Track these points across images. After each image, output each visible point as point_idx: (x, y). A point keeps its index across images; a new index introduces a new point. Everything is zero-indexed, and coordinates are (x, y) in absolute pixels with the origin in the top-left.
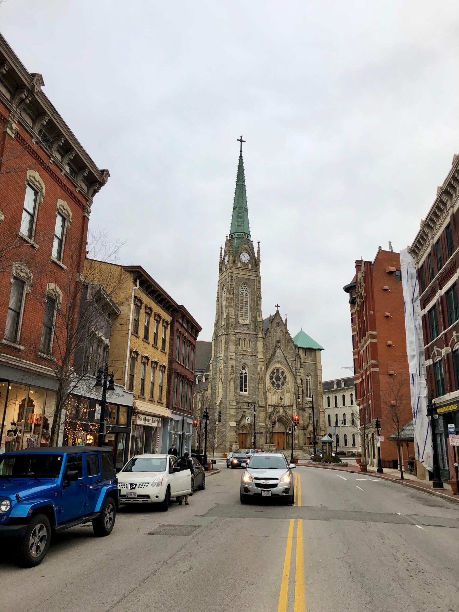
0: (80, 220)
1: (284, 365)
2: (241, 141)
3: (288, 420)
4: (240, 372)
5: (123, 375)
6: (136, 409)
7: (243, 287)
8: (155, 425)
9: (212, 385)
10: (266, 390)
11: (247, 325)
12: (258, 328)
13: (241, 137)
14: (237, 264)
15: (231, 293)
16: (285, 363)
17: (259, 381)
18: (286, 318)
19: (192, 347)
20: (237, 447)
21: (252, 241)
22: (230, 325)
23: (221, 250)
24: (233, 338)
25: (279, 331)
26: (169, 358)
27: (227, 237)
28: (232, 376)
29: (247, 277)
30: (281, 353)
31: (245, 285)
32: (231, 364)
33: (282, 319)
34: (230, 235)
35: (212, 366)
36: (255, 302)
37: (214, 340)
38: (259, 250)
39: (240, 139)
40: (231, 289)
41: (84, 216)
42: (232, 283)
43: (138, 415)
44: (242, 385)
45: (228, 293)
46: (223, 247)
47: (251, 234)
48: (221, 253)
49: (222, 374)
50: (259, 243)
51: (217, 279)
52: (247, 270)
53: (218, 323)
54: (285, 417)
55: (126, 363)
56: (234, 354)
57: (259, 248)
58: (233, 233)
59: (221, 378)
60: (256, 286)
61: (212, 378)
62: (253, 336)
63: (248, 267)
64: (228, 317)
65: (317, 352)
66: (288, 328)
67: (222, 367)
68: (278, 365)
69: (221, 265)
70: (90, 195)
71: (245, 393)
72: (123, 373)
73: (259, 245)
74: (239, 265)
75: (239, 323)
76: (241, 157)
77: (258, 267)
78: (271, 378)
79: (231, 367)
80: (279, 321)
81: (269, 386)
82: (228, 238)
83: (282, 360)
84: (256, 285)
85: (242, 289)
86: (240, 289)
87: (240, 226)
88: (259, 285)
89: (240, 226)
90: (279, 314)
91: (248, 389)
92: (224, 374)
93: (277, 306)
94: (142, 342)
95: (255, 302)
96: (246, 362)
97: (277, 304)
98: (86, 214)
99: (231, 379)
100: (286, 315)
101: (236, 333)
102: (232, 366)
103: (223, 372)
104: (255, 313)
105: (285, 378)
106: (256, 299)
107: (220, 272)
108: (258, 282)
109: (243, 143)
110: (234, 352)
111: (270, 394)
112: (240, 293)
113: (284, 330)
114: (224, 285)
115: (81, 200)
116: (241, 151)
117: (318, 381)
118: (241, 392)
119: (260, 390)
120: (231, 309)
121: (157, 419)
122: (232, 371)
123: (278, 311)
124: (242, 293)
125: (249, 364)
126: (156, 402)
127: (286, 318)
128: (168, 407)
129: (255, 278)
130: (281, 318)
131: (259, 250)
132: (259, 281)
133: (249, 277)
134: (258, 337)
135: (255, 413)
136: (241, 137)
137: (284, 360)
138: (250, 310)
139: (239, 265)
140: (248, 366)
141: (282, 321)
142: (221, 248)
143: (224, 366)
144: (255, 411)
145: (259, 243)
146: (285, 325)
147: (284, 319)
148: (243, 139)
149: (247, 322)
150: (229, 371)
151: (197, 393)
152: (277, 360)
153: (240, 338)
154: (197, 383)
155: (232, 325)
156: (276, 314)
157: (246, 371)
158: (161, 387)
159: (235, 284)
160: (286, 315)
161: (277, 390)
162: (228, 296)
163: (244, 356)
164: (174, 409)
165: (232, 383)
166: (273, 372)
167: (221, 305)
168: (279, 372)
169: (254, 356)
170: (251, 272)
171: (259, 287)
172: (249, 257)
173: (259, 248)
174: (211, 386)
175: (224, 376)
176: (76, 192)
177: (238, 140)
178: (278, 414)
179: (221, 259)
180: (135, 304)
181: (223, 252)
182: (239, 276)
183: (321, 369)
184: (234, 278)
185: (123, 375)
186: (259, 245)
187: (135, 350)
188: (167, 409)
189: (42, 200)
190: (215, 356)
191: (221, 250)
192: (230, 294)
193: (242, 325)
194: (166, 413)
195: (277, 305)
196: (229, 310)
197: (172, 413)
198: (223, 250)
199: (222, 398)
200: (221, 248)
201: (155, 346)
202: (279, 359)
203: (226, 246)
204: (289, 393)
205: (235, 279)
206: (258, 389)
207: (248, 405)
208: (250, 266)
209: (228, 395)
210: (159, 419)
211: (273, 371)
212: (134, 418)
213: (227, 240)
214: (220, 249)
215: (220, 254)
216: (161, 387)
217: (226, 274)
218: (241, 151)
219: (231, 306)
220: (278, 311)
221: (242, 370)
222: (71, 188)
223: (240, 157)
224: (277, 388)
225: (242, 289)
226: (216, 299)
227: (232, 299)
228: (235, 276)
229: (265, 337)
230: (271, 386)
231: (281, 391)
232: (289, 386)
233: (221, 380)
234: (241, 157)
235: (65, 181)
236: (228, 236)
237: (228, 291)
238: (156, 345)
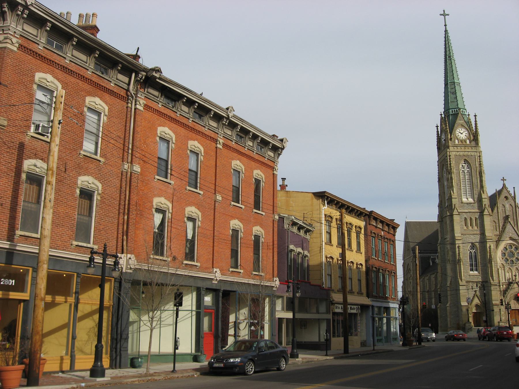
0: (272, 177)
2: (444, 15)
4: (469, 252)
5: (322, 276)
6: (334, 300)
7: (464, 165)
8: (354, 311)
10: (499, 268)
11: (471, 203)
13: (444, 11)
14: (454, 141)
18: (514, 191)
19: (392, 243)
21: (469, 115)
23: (437, 129)
26: (365, 257)
27: (441, 115)
29: (466, 153)
33: (510, 192)
34: (444, 112)
35: (440, 248)
38: (476, 124)
39: (442, 13)
41: (274, 174)
43: (336, 305)
44: (471, 265)
46: (439, 125)
47: (466, 108)
48: (438, 132)
50: (475, 116)
51: (437, 159)
52: (466, 146)
53: (442, 204)
55: (322, 267)
56: (460, 235)
58: (447, 110)
59: (449, 260)
63: (466, 143)
67: (449, 249)
69: (439, 144)
70: (276, 158)
72: (321, 275)
73: (475, 118)
74: (457, 141)
75: (462, 203)
76: (446, 31)
78: (504, 254)
80: (506, 195)
82: (443, 116)
85: (462, 167)
86: (460, 168)
90: (506, 189)
93: (503, 180)
94: (336, 248)
97: (503, 178)
98: (275, 172)
100: (514, 188)
101: (461, 213)
109: (446, 16)
110: (459, 233)
112: (461, 171)
114: (443, 164)
115: (270, 164)
116: (445, 25)
121: (355, 307)
123: (504, 185)
124: (463, 171)
126: (356, 293)
127: (514, 191)
128: (368, 296)
129: (476, 154)
130: (509, 192)
131: (476, 124)
133: (469, 154)
135: (485, 292)
136: (444, 11)
139: (457, 141)
141: (510, 195)
142: (437, 127)
144: (484, 290)
145: (475, 116)
147: (512, 192)
148: (446, 13)
149: (471, 200)
154: (431, 264)
156: (503, 188)
158: (360, 280)
159: (454, 162)
160: (514, 188)
163: (470, 235)
164: (376, 297)
166: (506, 248)
167: (443, 186)
168: (512, 248)
170: (470, 148)
173: (476, 121)
174: (440, 268)
176: (265, 161)
177: (441, 15)
179: (438, 138)
180: (325, 220)
181: (439, 130)
182: (458, 154)
185: (322, 276)
186: (475, 118)
187: (329, 256)
188: (367, 298)
189: (243, 176)
190: (442, 238)
191: (437, 129)
193: (466, 204)
194: (366, 301)
197: (373, 301)
198: (439, 128)
199: (451, 280)
201: (351, 250)
203: (441, 125)
205: (454, 157)
207: (477, 285)
208: (468, 142)
210: (358, 307)
211: (505, 247)
212: (332, 307)
213: (442, 118)
214: (436, 128)
215: (436, 133)
216: (360, 280)
217: (444, 153)
218: (445, 25)
220: (504, 185)
221: (471, 249)
222: (261, 159)
223: (445, 31)
224: (510, 265)
225: (462, 167)
226: (437, 180)
229: (492, 214)
230: (504, 263)
234: (446, 31)
235: (257, 157)
236: (443, 114)
238: (351, 248)
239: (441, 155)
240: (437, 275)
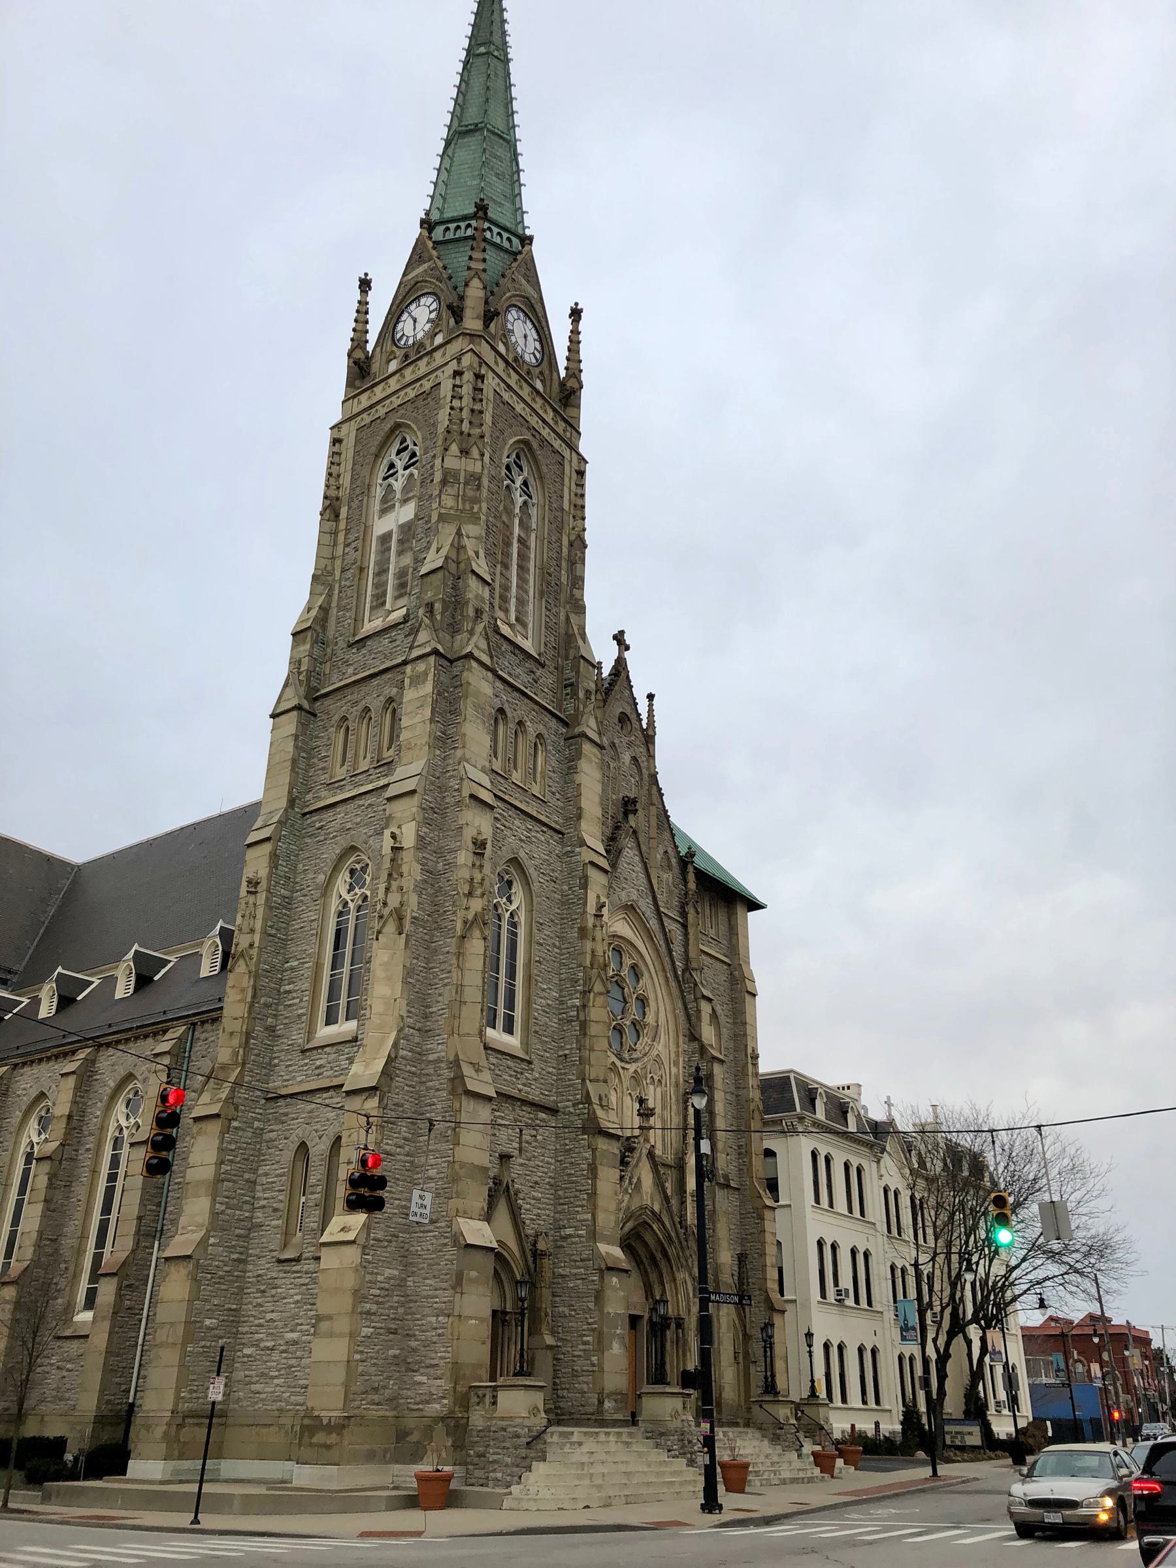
9: (257, 976)
12: (581, 695)
15: (475, 453)
17: (588, 980)
20: (534, 1411)
22: (471, 612)
24: (480, 684)
25: (626, 758)
28: (477, 905)
29: (534, 421)
30: (639, 868)
31: (524, 463)
32: (469, 834)
36: (564, 564)
37: (298, 708)
40: (476, 431)
42: (477, 407)
45: (454, 448)
48: (363, 310)
49: (408, 883)
50: (576, 314)
53: (324, 628)
57: (575, 332)
60: (566, 491)
61: (264, 933)
62: (553, 723)
64: (452, 567)
65: (740, 910)
68: (622, 927)
71: (506, 1038)
77: (571, 412)
79: (471, 846)
80: (628, 710)
84: (566, 480)
87: (501, 205)
88: (579, 491)
89: (501, 205)
91: (518, 1014)
92: (419, 889)
93: (619, 638)
95: (564, 564)
96: (522, 854)
99: (468, 925)
102: (479, 846)
103: (412, 869)
104: (562, 617)
105: (643, 1001)
106: (565, 550)
107: (350, 384)
108: (574, 475)
113: (642, 759)
117: (750, 1051)
118: (490, 1032)
119: (594, 1029)
120: (471, 529)
122: (478, 877)
125: (536, 867)
132: (581, 474)
134: (574, 738)
137: (645, 906)
138: (542, 594)
140: (527, 882)
142: (365, 284)
143: (420, 838)
145: (576, 314)
146: (648, 738)
147: (643, 708)
150: (465, 873)
151: (16, 1065)
153: (501, 711)
155: (479, 612)
157: (513, 907)
162: (452, 463)
165: (476, 946)
169: (556, 837)
170: (551, 414)
171: (579, 502)
172: (538, 345)
173: (575, 332)
174: (247, 982)
175: (413, 899)
182: (506, 396)
183: (754, 995)
184: (488, 393)
192: (465, 452)
193: (505, 646)
196: (459, 533)
199: (395, 1045)
200: (365, 284)
204: (659, 1090)
205: (491, 396)
206: (584, 1026)
209: (440, 1022)
219: (475, 518)
226: (318, 504)
227: (474, 479)
228: (491, 382)
231: (632, 1068)
232: (660, 1048)
233: (391, 927)
237: (455, 435)
239: (365, 400)
240: (94, 1062)
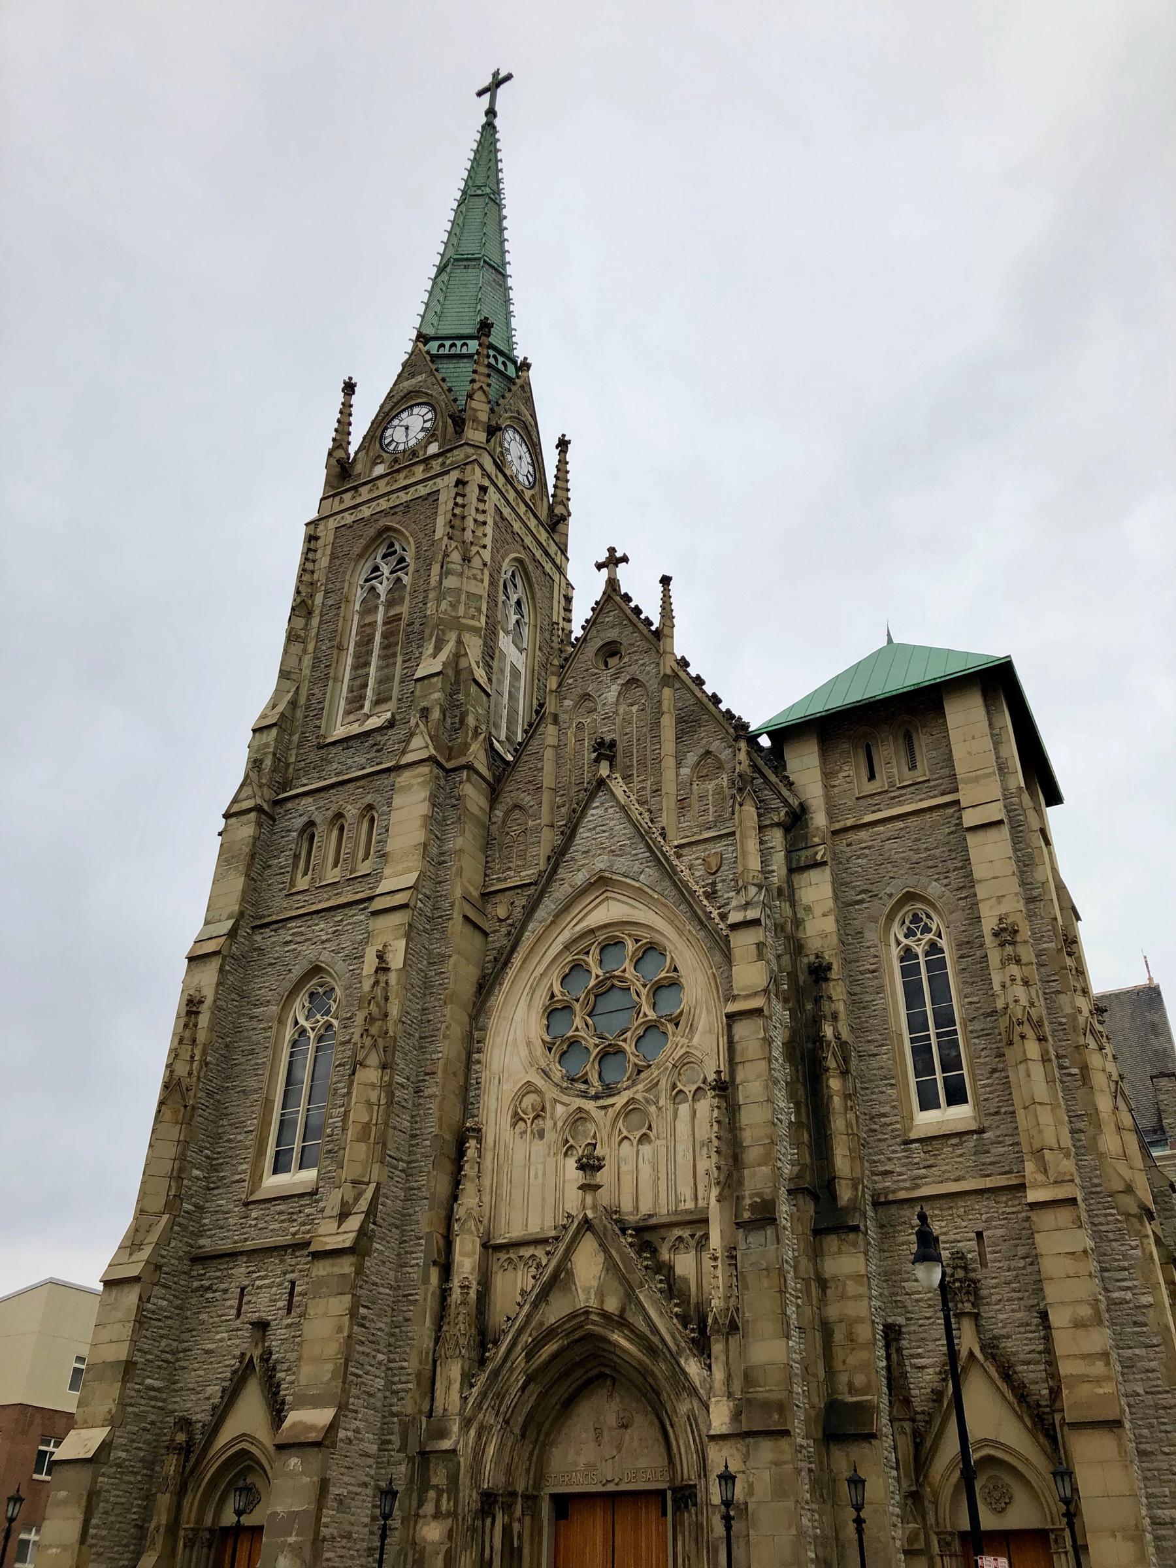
1: (640, 895)
3: (652, 1350)
16: (649, 875)
54: (620, 1322)
66: (682, 644)
81: (529, 1088)
83: (622, 864)
100: (666, 581)
111: (539, 1147)
123: (612, 584)
152: (580, 878)
160: (666, 581)
161: (589, 1105)
178: (555, 1312)
195: (619, 555)
202: (601, 863)
220: (612, 584)
